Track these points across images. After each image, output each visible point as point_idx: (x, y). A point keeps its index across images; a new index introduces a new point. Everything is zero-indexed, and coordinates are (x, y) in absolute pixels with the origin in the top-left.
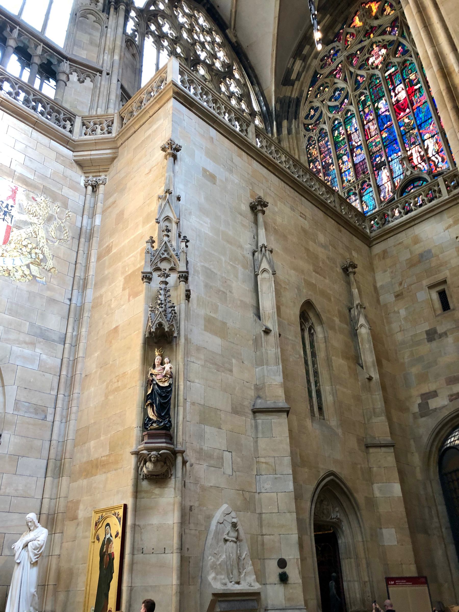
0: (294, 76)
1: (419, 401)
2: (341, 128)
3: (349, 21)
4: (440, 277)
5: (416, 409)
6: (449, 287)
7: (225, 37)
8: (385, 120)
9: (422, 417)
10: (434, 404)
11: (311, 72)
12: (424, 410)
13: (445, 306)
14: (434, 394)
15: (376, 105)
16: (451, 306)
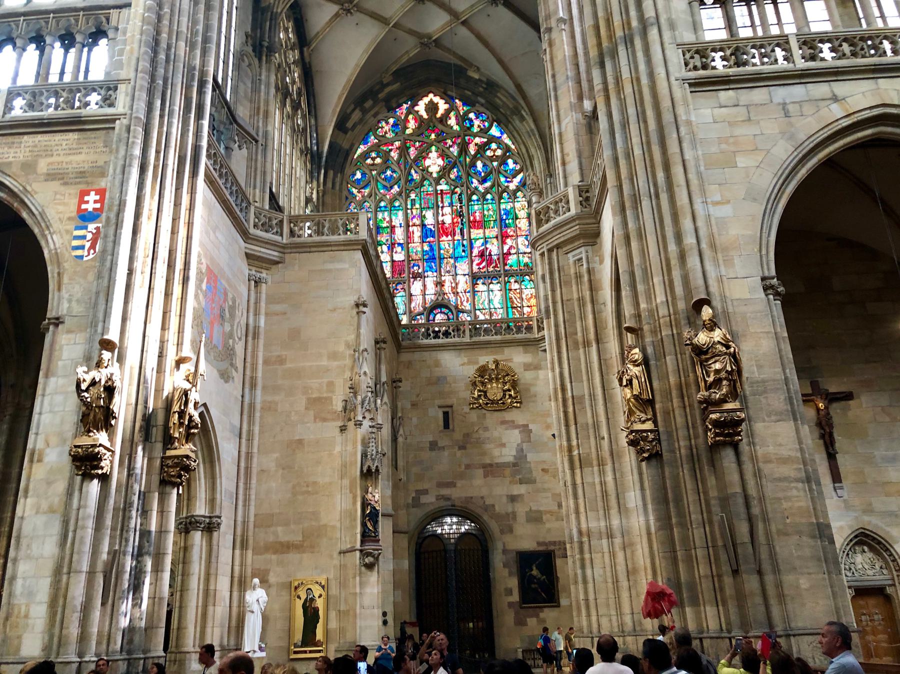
0: (349, 124)
1: (414, 495)
2: (386, 214)
3: (415, 99)
4: (449, 402)
5: (410, 501)
6: (453, 412)
7: (302, 53)
8: (429, 233)
9: (413, 507)
10: (424, 499)
11: (366, 129)
12: (416, 503)
13: (446, 425)
14: (425, 492)
15: (424, 212)
16: (451, 427)
